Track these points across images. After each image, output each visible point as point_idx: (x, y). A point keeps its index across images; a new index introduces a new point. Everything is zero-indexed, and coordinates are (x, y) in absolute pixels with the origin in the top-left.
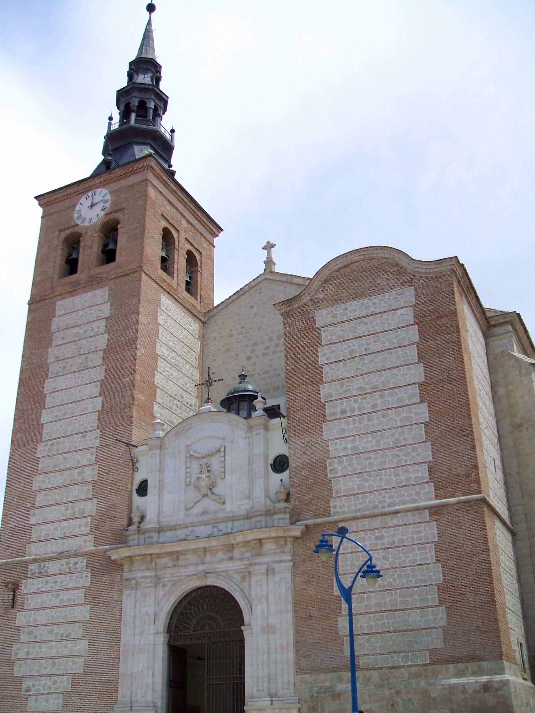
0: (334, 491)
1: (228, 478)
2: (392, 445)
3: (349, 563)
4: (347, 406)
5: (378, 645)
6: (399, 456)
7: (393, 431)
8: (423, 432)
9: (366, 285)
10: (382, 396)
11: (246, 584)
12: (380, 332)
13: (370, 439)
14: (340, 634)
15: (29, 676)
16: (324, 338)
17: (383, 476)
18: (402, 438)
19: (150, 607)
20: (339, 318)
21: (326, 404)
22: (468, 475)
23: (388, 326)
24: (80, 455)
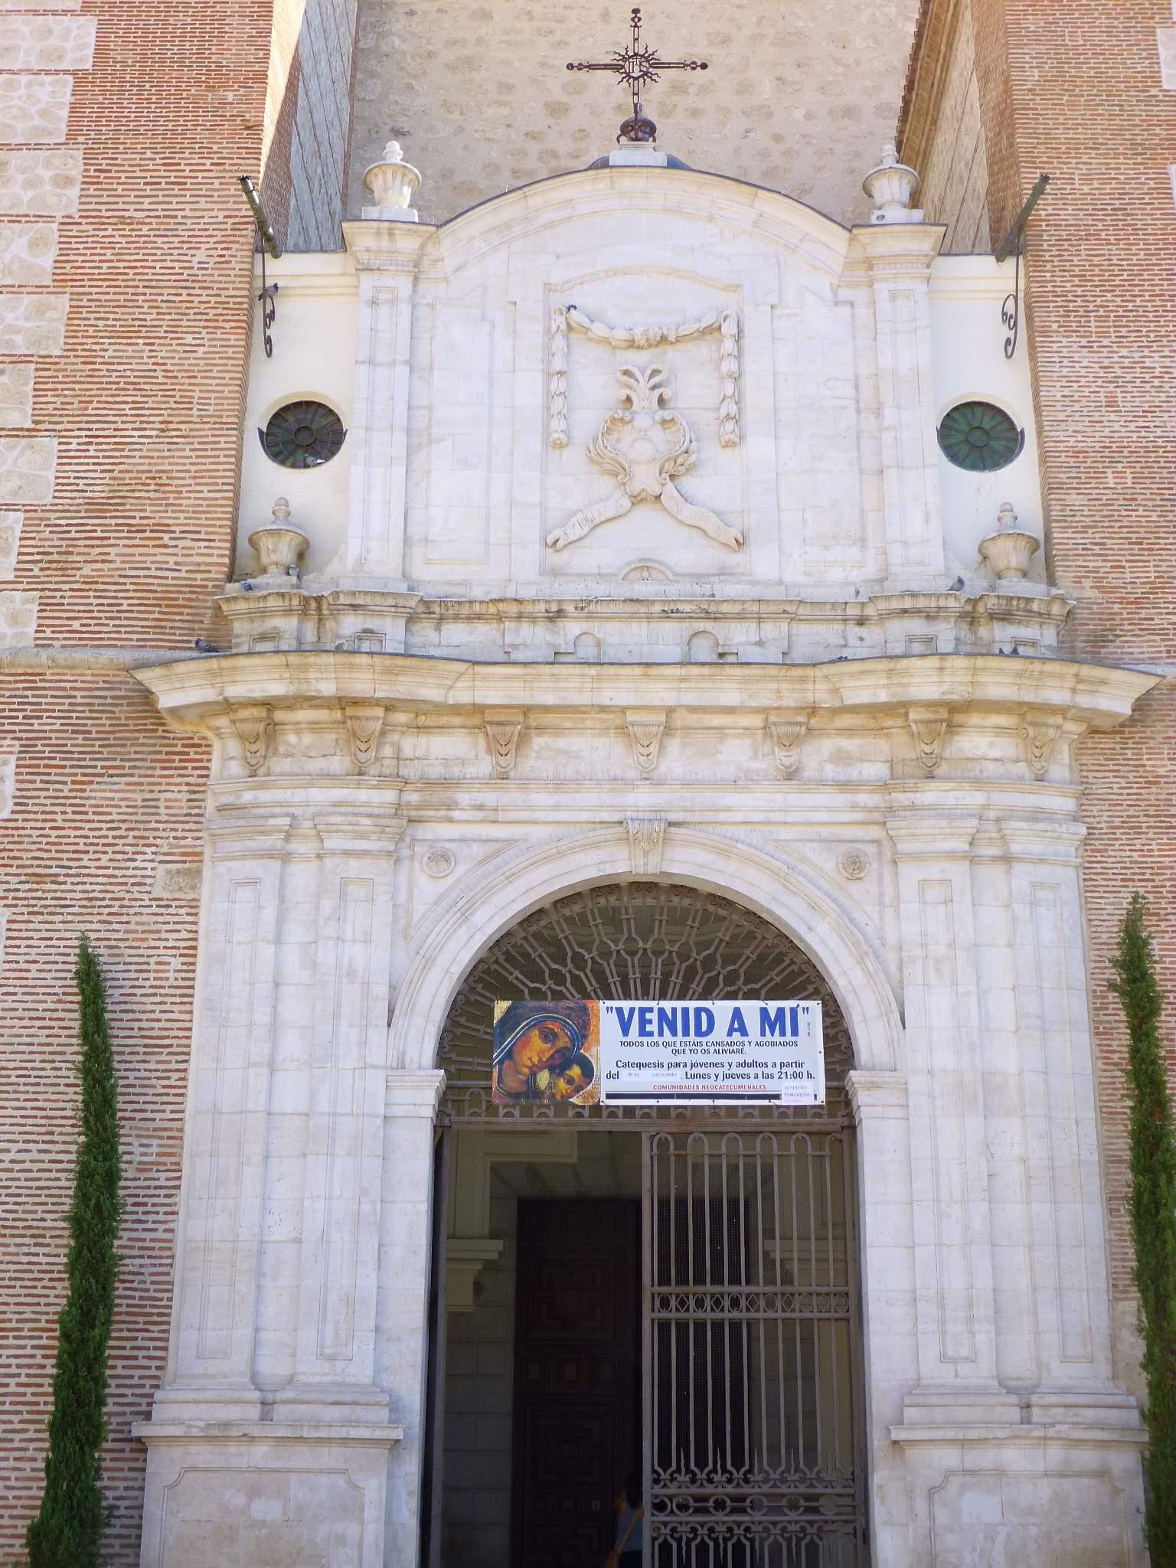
1: (759, 446)
11: (863, 892)
19: (368, 941)
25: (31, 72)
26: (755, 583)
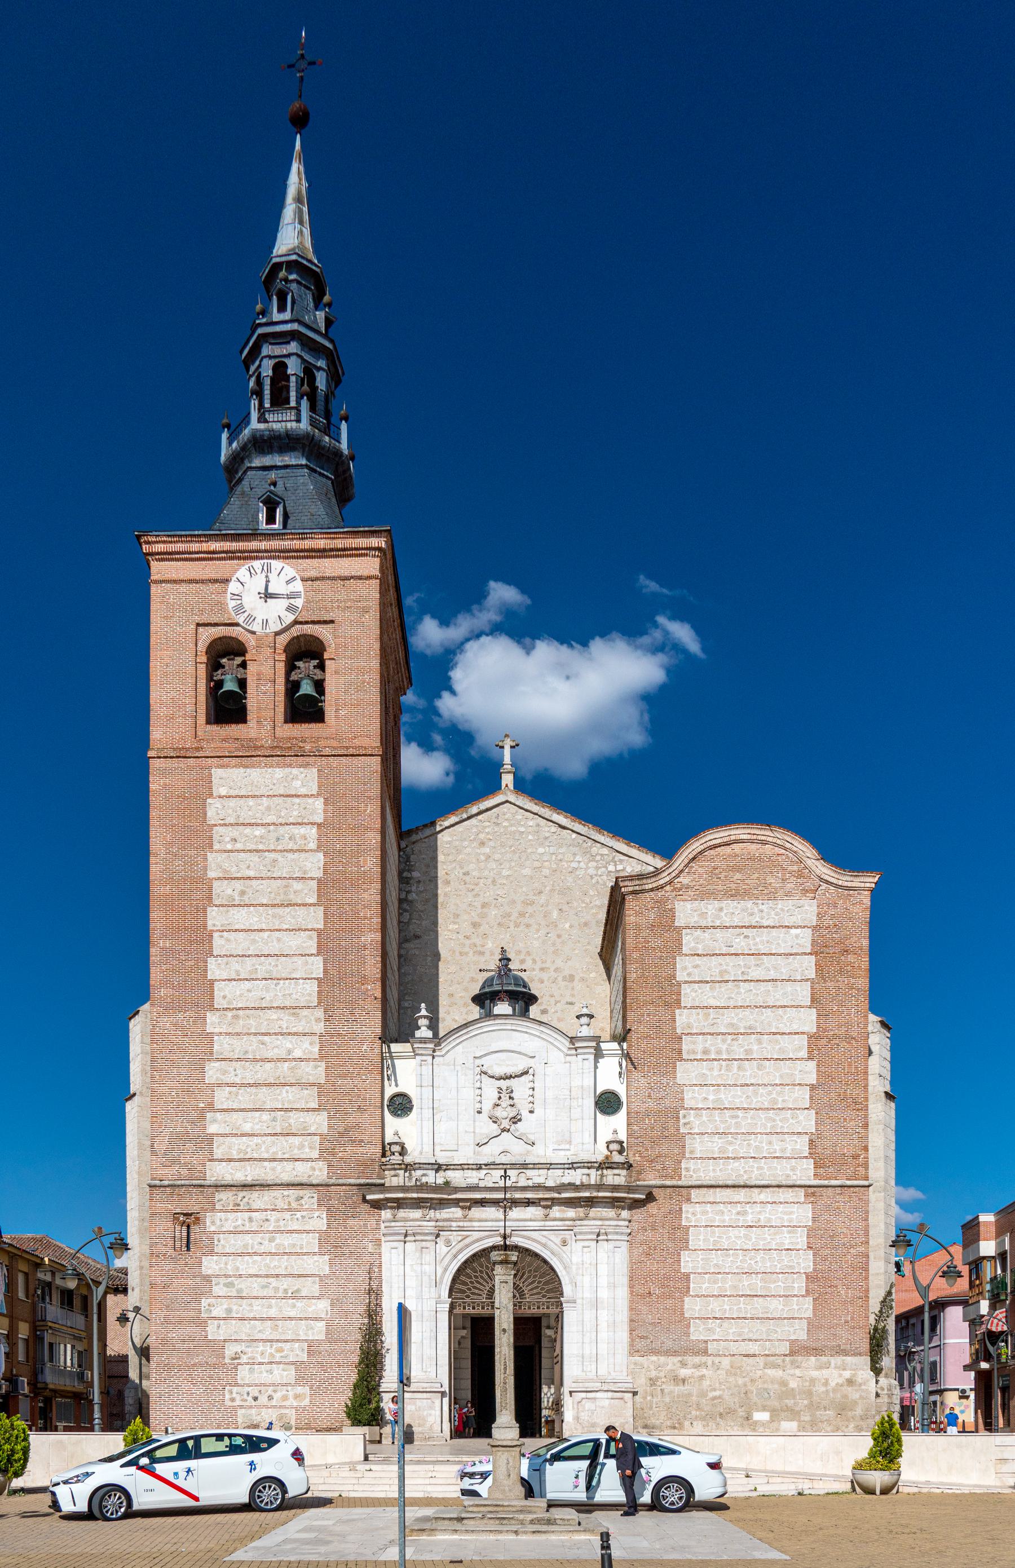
0: (687, 1150)
3: (702, 1237)
4: (711, 1045)
5: (731, 1331)
6: (774, 1120)
7: (770, 1088)
8: (808, 1097)
9: (752, 881)
10: (760, 1042)
12: (765, 954)
13: (739, 1093)
14: (686, 1315)
15: (236, 1341)
17: (752, 1142)
18: (780, 1099)
20: (709, 920)
21: (684, 1037)
22: (856, 1157)
23: (776, 948)
24: (291, 1042)
25: (303, 979)
26: (538, 1156)
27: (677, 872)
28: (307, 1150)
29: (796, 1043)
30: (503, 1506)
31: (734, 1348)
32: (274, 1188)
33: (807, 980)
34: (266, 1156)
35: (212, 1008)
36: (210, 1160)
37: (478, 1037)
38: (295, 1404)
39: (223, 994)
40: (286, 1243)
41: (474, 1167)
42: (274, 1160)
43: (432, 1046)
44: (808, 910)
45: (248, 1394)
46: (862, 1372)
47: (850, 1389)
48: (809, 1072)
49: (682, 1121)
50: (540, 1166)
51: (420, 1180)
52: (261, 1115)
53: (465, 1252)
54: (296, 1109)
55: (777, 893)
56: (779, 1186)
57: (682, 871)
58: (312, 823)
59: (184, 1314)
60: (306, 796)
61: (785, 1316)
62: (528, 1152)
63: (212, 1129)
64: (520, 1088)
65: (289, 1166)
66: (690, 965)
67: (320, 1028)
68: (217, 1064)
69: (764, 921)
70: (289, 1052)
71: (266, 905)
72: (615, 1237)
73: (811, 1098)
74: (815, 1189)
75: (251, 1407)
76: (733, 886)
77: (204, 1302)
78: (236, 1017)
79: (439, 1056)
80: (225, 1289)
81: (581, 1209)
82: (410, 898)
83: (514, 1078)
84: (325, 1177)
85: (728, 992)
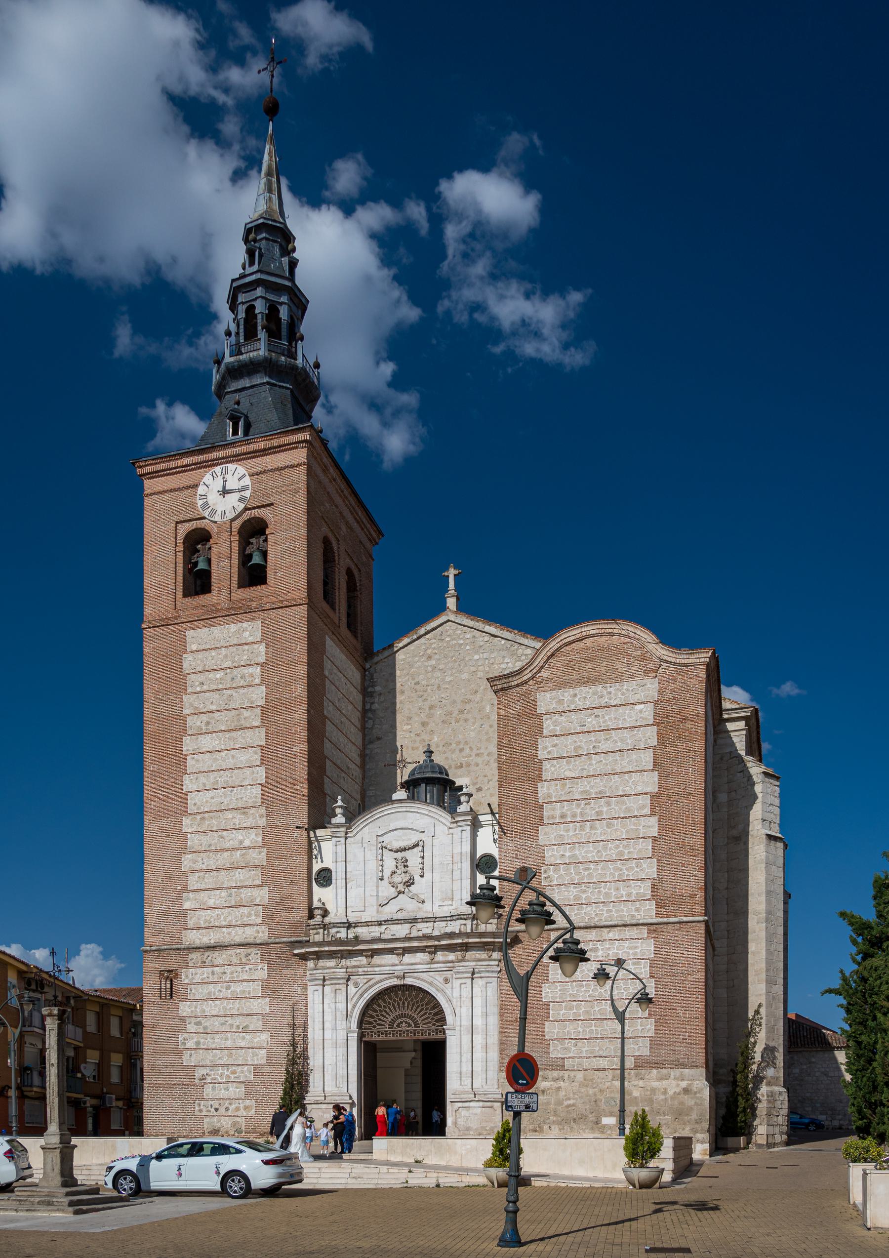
2: (614, 857)
5: (584, 1049)
6: (621, 870)
7: (618, 843)
10: (609, 804)
12: (613, 729)
13: (591, 849)
14: (546, 1037)
15: (203, 1066)
16: (546, 727)
17: (602, 889)
18: (626, 851)
20: (566, 705)
21: (545, 805)
24: (242, 834)
25: (250, 785)
27: (537, 668)
28: (253, 917)
29: (640, 802)
30: (36, 1191)
31: (586, 1063)
32: (230, 948)
33: (650, 748)
34: (224, 923)
35: (186, 813)
36: (185, 929)
37: (380, 819)
38: (245, 1114)
39: (196, 801)
40: (238, 990)
41: (376, 923)
42: (230, 926)
43: (344, 829)
44: (651, 688)
45: (211, 1106)
46: (698, 1082)
47: (686, 1097)
48: (652, 826)
49: (543, 876)
50: (427, 920)
51: (335, 936)
52: (221, 892)
53: (369, 992)
54: (246, 886)
55: (623, 676)
56: (625, 925)
57: (542, 667)
58: (257, 664)
59: (168, 1046)
60: (253, 643)
61: (630, 1035)
62: (419, 909)
63: (187, 905)
64: (413, 857)
65: (240, 931)
66: (549, 745)
67: (262, 822)
68: (190, 856)
69: (612, 701)
70: (241, 842)
71: (224, 731)
72: (487, 975)
73: (653, 848)
74: (657, 926)
75: (213, 1116)
76: (586, 675)
77: (181, 1037)
78: (203, 819)
79: (351, 837)
80: (195, 1027)
81: (459, 953)
82: (373, 707)
83: (408, 850)
84: (266, 938)
85: (582, 764)
